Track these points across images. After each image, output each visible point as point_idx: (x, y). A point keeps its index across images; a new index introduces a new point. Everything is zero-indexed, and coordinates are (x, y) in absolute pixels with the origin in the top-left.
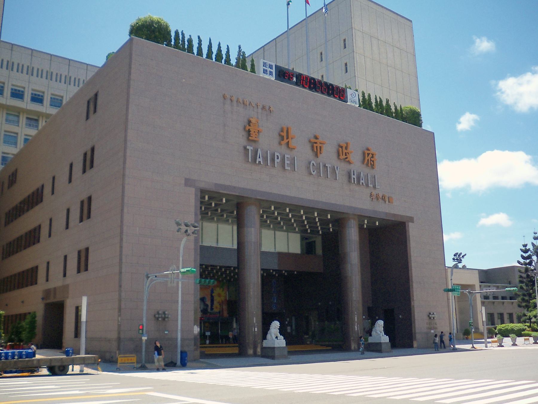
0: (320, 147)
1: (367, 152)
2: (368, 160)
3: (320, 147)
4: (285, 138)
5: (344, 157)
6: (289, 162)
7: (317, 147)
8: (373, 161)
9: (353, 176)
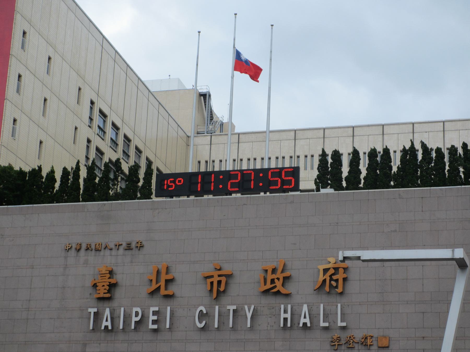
0: (219, 282)
1: (321, 267)
2: (324, 281)
3: (219, 282)
4: (154, 282)
5: (269, 286)
6: (155, 318)
7: (212, 283)
8: (337, 281)
9: (283, 316)
